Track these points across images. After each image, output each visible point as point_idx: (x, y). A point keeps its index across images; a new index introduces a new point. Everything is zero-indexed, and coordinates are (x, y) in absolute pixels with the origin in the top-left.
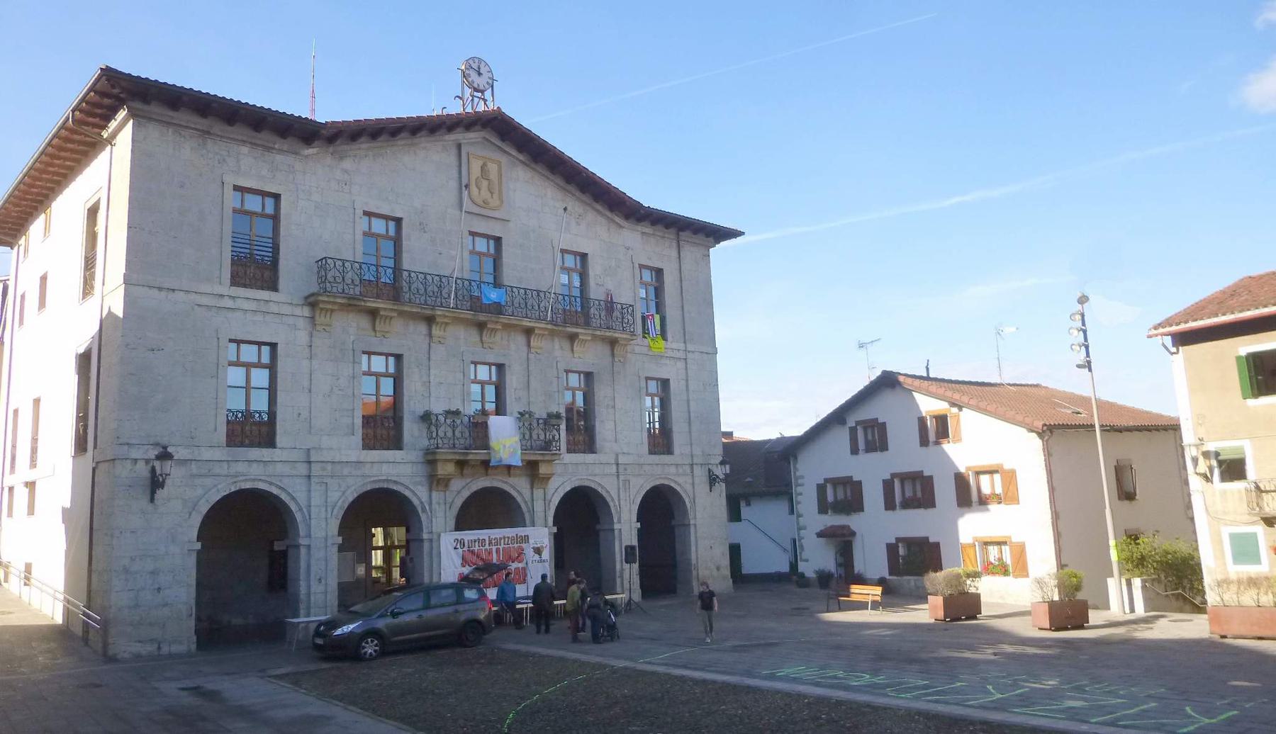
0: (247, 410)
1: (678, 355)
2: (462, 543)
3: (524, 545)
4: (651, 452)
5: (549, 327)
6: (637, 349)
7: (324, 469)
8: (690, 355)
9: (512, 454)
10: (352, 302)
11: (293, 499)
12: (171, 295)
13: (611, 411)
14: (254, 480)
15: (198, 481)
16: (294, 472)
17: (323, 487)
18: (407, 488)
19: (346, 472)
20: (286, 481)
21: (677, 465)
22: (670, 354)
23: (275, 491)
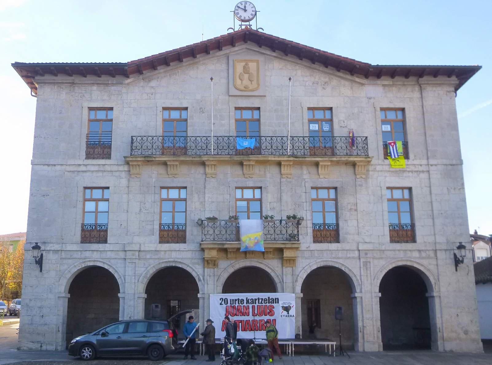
1: (421, 169)
2: (226, 301)
3: (274, 305)
4: (392, 241)
5: (292, 159)
6: (379, 168)
7: (133, 255)
8: (432, 168)
9: (257, 243)
10: (149, 159)
11: (116, 271)
12: (53, 168)
13: (354, 213)
14: (94, 261)
15: (65, 261)
16: (116, 257)
17: (134, 265)
18: (188, 266)
19: (148, 257)
20: (112, 261)
21: (420, 251)
22: (412, 168)
23: (106, 267)
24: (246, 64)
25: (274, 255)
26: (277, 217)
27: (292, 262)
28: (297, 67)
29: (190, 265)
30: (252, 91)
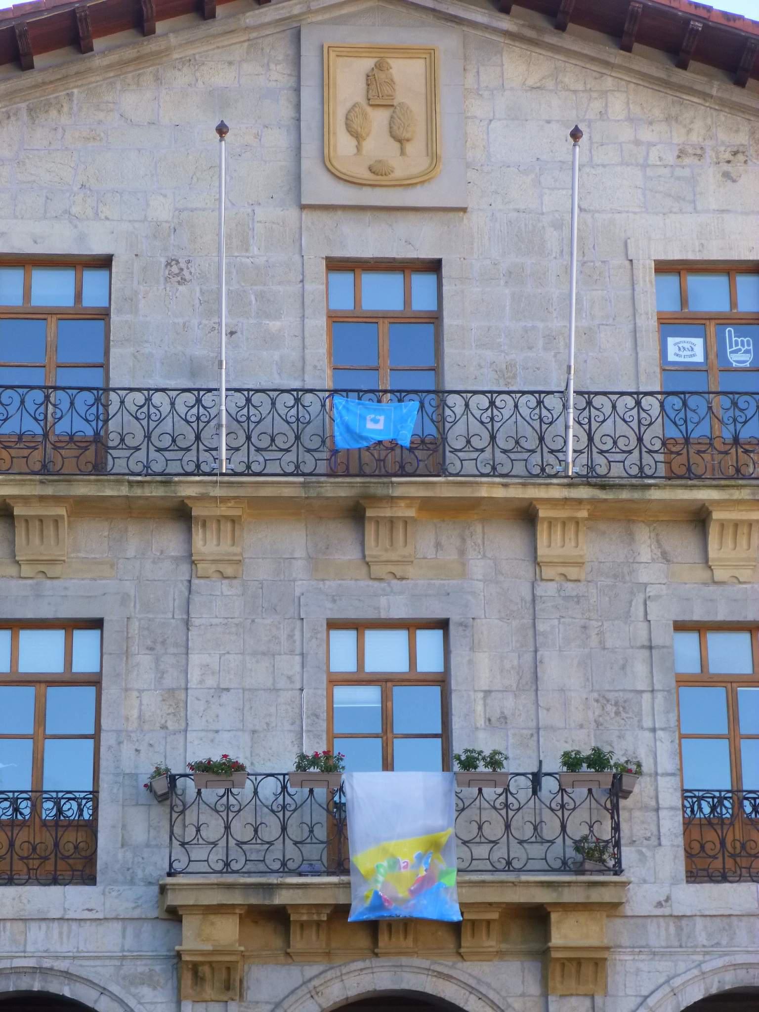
0: (37, 794)
5: (583, 493)
9: (424, 884)
18: (104, 991)
24: (380, 66)
25: (504, 937)
26: (519, 762)
27: (588, 970)
28: (609, 82)
29: (114, 989)
30: (407, 184)
